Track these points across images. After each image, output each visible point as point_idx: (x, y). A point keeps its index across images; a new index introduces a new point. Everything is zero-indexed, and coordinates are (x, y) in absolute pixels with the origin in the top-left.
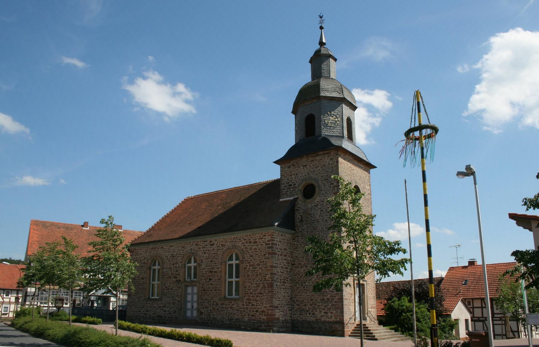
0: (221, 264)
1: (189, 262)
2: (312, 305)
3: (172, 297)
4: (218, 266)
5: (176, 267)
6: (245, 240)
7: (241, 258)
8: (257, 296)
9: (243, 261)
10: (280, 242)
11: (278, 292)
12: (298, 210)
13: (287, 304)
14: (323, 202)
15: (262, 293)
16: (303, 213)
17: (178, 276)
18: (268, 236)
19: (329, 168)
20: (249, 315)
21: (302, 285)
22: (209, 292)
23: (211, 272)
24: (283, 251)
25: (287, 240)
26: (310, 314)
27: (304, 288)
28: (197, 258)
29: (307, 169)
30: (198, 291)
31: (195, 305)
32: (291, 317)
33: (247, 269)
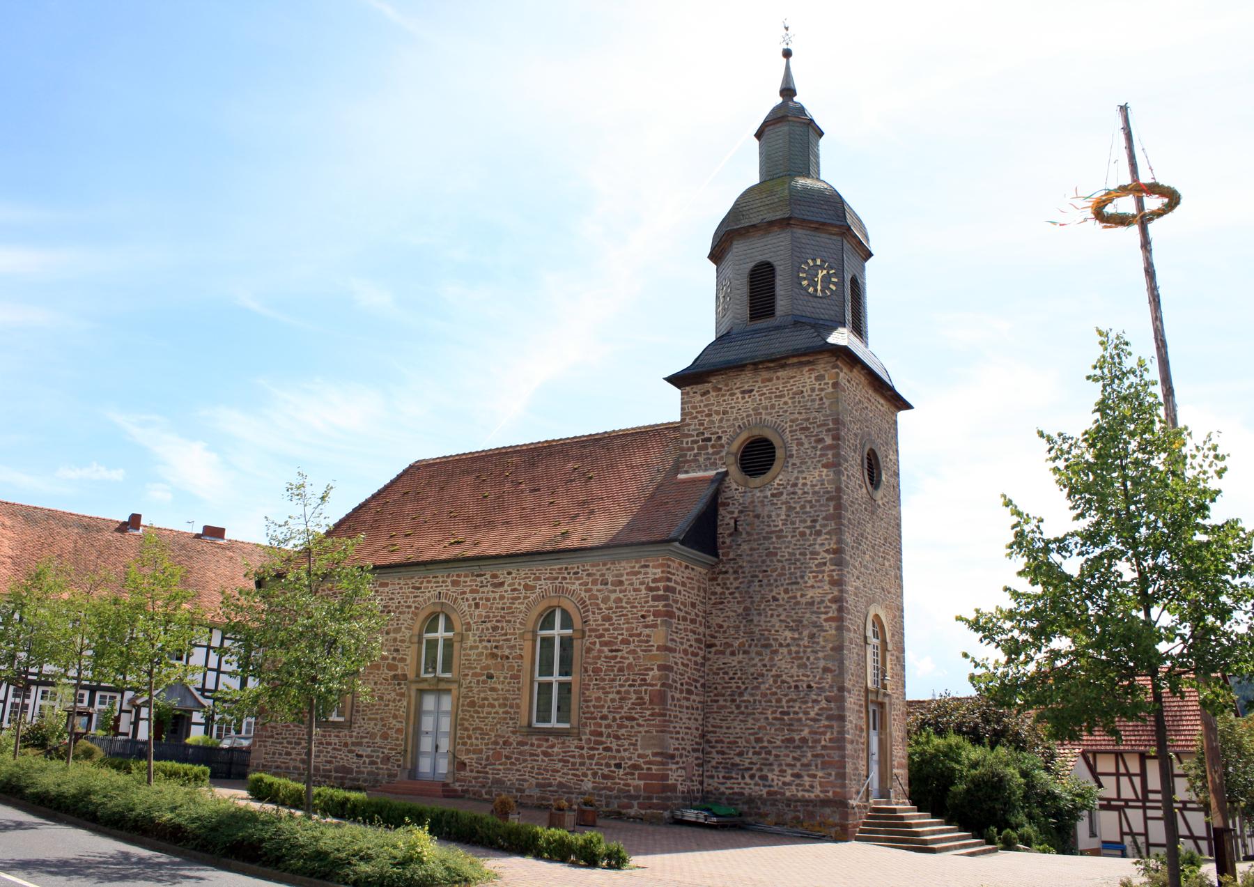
0: (522, 636)
1: (433, 627)
2: (758, 753)
3: (382, 719)
4: (512, 643)
5: (395, 640)
6: (588, 575)
7: (577, 623)
8: (620, 726)
9: (583, 632)
10: (684, 584)
11: (676, 717)
12: (726, 505)
13: (694, 750)
14: (795, 485)
15: (634, 719)
16: (741, 512)
17: (400, 665)
18: (654, 567)
19: (813, 400)
20: (595, 775)
21: (733, 701)
22: (486, 709)
23: (494, 656)
24: (689, 609)
25: (698, 581)
26: (752, 777)
27: (738, 707)
28: (454, 617)
29: (754, 400)
30: (456, 706)
31: (445, 745)
32: (701, 783)
33: (595, 653)
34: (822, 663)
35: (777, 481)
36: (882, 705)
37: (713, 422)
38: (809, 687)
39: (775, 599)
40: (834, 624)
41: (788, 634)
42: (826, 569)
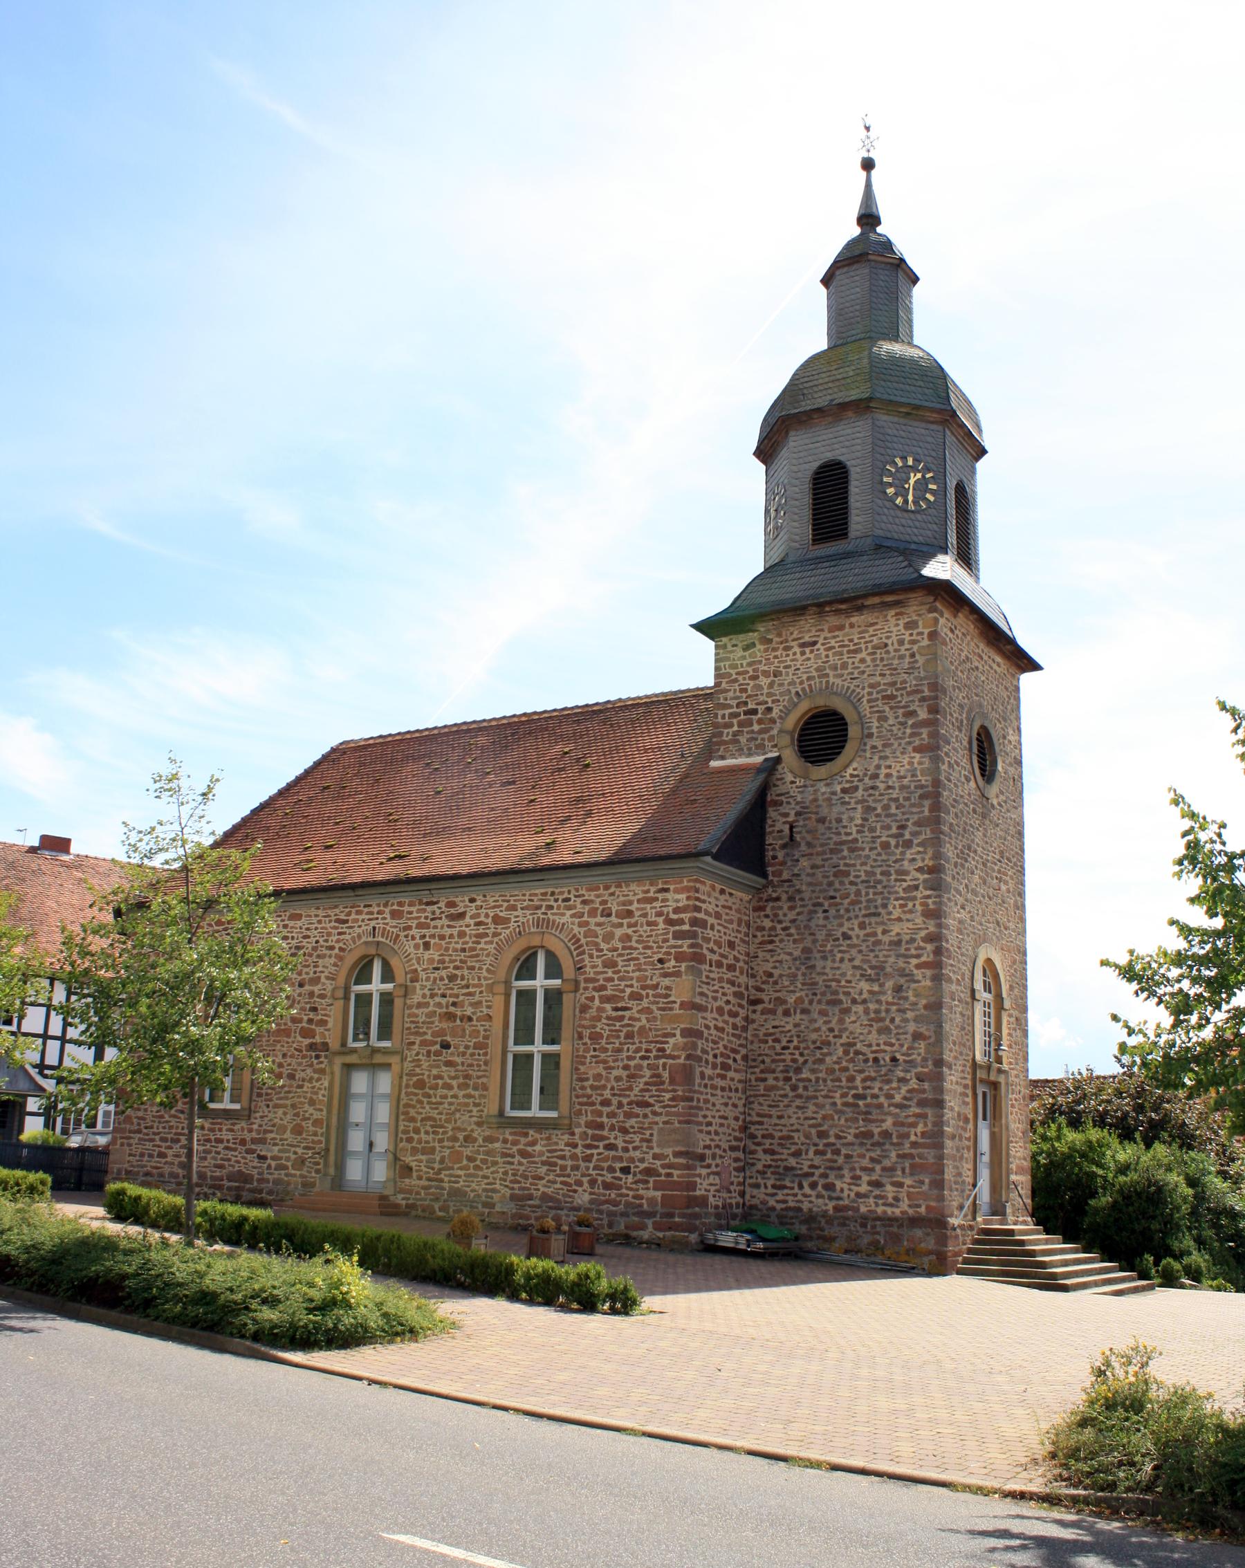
0: (490, 988)
1: (364, 976)
2: (823, 1153)
3: (293, 1106)
4: (477, 998)
5: (311, 994)
6: (584, 902)
7: (569, 972)
8: (628, 1115)
9: (577, 983)
10: (718, 916)
11: (706, 1101)
12: (777, 804)
13: (733, 1149)
14: (875, 776)
15: (648, 1105)
16: (798, 814)
17: (319, 1030)
18: (677, 891)
19: (901, 657)
20: (593, 1182)
21: (788, 1079)
22: (440, 1092)
23: (450, 1017)
24: (725, 950)
25: (738, 911)
26: (813, 1186)
27: (794, 1088)
28: (395, 962)
29: (818, 657)
30: (398, 1087)
31: (382, 1141)
32: (742, 1194)
33: (593, 1012)
34: (911, 1027)
35: (850, 771)
36: (995, 1086)
37: (760, 687)
38: (894, 1059)
39: (846, 937)
40: (928, 973)
41: (865, 986)
42: (918, 894)
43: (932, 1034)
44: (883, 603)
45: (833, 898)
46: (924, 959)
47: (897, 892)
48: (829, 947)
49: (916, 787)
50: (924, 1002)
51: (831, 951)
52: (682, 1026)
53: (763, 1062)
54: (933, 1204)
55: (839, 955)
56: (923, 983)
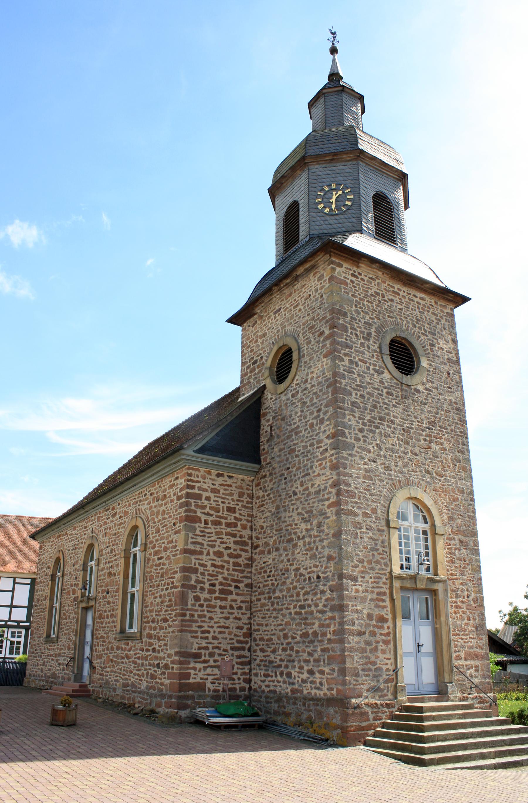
10: (214, 491)
14: (306, 381)
26: (281, 674)
34: (326, 552)
35: (295, 382)
36: (434, 592)
37: (258, 346)
38: (318, 577)
39: (295, 494)
40: (334, 509)
41: (303, 526)
42: (327, 454)
43: (337, 555)
44: (306, 270)
45: (288, 468)
46: (331, 500)
47: (317, 456)
48: (287, 503)
49: (325, 381)
50: (332, 532)
51: (288, 505)
52: (180, 565)
53: (259, 587)
54: (340, 687)
55: (292, 507)
56: (331, 519)
